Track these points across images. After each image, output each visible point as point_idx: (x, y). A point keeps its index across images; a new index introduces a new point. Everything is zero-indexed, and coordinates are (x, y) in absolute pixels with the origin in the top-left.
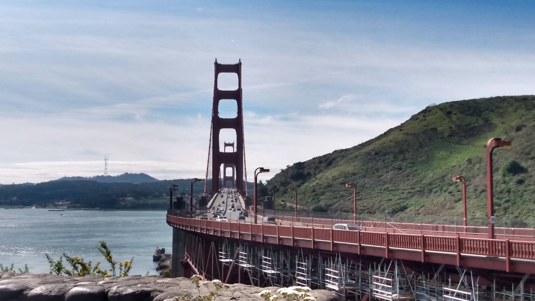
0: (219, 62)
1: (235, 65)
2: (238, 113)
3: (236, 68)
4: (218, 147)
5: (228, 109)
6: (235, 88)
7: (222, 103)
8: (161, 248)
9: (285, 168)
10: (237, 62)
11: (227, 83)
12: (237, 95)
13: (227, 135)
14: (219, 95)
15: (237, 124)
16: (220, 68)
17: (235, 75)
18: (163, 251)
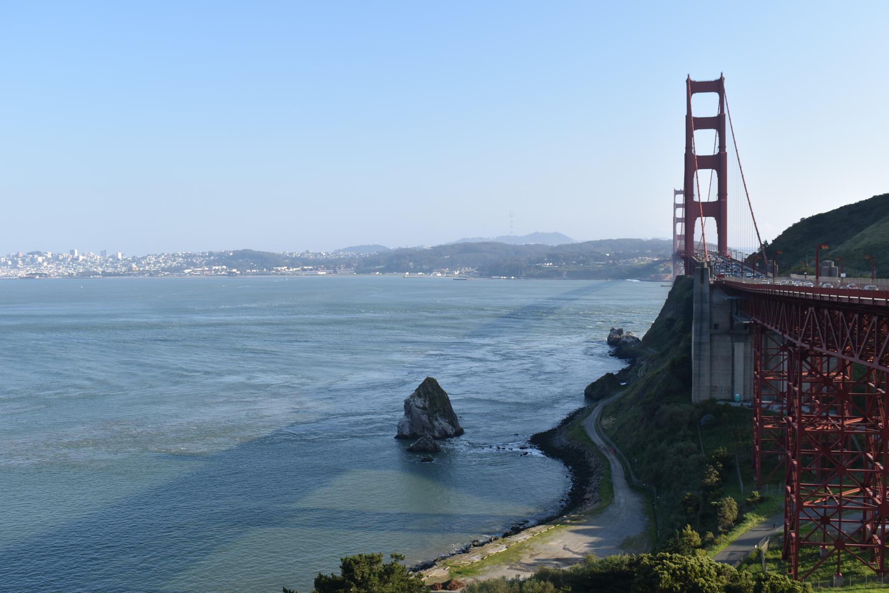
0: (693, 78)
1: (716, 81)
2: (719, 147)
3: (717, 86)
4: (692, 195)
5: (706, 143)
6: (714, 113)
7: (698, 134)
8: (617, 329)
9: (798, 221)
10: (718, 77)
11: (706, 105)
12: (718, 123)
13: (706, 180)
14: (693, 124)
15: (718, 162)
16: (694, 87)
17: (715, 96)
18: (620, 332)
